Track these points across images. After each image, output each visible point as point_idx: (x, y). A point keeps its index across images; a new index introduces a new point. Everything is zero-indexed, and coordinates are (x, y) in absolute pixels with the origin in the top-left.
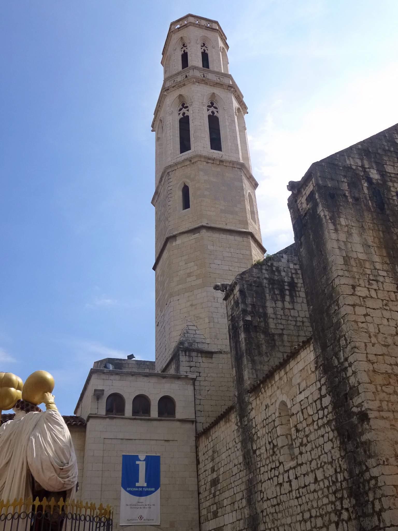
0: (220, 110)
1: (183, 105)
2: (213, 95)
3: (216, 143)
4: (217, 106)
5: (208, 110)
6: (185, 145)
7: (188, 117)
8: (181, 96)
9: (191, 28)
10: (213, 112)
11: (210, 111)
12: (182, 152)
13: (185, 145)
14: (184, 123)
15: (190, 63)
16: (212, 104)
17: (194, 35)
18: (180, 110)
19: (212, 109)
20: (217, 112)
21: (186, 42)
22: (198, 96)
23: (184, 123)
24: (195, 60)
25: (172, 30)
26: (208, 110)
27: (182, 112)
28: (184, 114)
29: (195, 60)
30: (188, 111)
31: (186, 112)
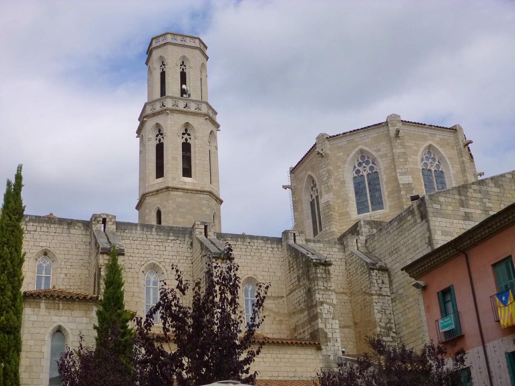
0: (192, 136)
1: (159, 131)
2: (187, 124)
3: (187, 172)
4: (190, 133)
5: (183, 137)
6: (160, 172)
7: (162, 144)
8: (158, 125)
9: (170, 47)
10: (186, 139)
11: (184, 138)
12: (157, 178)
13: (160, 172)
14: (160, 149)
15: (168, 93)
16: (186, 130)
17: (173, 57)
18: (157, 136)
19: (186, 136)
20: (190, 138)
21: (165, 63)
22: (173, 125)
23: (160, 149)
24: (173, 86)
25: (154, 45)
26: (183, 137)
27: (158, 138)
28: (160, 140)
29: (173, 86)
30: (163, 138)
31: (162, 139)
